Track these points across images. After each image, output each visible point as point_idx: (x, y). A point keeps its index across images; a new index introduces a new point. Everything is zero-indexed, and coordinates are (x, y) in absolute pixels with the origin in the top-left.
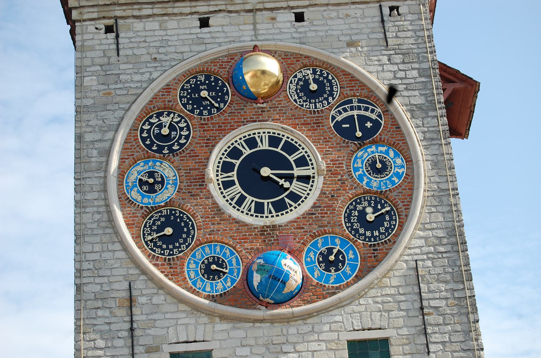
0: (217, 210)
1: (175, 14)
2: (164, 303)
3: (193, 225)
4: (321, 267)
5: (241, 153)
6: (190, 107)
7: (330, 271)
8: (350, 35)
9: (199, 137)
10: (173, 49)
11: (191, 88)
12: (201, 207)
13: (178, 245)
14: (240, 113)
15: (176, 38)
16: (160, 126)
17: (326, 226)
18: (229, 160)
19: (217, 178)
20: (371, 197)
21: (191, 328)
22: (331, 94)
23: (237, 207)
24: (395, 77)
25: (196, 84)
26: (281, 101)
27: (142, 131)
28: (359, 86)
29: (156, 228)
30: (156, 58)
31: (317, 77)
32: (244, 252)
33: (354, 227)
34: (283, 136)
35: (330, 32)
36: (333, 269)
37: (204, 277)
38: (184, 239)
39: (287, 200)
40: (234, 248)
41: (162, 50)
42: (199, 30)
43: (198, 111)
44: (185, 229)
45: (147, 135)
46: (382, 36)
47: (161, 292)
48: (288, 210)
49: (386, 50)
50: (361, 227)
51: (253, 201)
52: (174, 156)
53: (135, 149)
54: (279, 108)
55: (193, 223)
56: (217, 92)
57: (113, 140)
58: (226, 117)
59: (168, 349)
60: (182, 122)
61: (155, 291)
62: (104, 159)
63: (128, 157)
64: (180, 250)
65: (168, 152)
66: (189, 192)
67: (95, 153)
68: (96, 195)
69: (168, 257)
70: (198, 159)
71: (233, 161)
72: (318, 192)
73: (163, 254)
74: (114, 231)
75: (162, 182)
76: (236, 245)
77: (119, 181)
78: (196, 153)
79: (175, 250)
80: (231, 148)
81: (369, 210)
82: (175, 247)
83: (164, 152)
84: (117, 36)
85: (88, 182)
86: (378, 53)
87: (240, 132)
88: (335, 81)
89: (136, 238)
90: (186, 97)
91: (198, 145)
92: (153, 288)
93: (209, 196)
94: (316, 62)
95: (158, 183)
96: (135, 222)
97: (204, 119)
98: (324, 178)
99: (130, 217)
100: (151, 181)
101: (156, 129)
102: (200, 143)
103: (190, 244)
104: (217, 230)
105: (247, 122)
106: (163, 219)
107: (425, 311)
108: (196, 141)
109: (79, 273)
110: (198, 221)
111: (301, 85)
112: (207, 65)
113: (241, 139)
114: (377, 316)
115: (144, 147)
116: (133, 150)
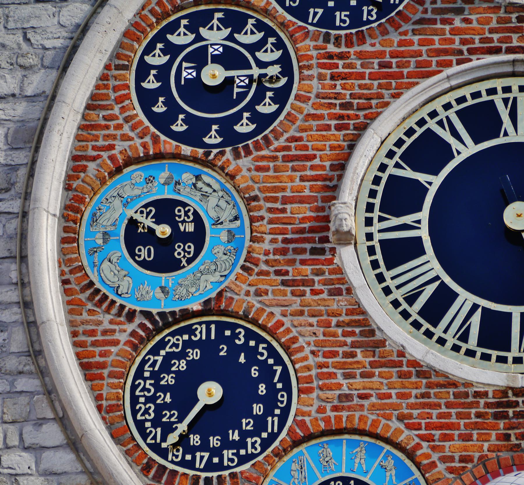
0: (362, 333)
3: (285, 377)
5: (447, 153)
9: (318, 96)
12: (314, 320)
13: (236, 437)
14: (449, 22)
16: (199, 58)
18: (408, 173)
19: (369, 229)
23: (426, 325)
27: (143, 70)
32: (441, 467)
38: (256, 418)
40: (411, 455)
43: (320, 11)
44: (262, 389)
45: (156, 85)
51: (475, 307)
52: (237, 155)
53: (119, 127)
55: (285, 370)
57: (53, 97)
58: (405, 33)
60: (269, 46)
62: (22, 157)
63: (95, 153)
64: (243, 452)
66: (278, 273)
69: (204, 475)
70: (312, 168)
71: (422, 177)
73: (191, 465)
74: (44, 385)
75: (198, 238)
76: (418, 446)
77: (66, 229)
78: (306, 148)
80: (416, 136)
82: (227, 444)
83: (206, 140)
87: (447, 85)
89: (107, 410)
91: (314, 123)
93: (340, 286)
95: (185, 237)
96: (109, 359)
97: (338, 38)
99: (95, 344)
100: (163, 231)
101: (185, 65)
102: (320, 117)
103: (273, 436)
104: (362, 397)
105: (471, 51)
106: (195, 354)
108: (308, 108)
110: (305, 361)
113: (447, 106)
115: (147, 123)
116: (112, 131)
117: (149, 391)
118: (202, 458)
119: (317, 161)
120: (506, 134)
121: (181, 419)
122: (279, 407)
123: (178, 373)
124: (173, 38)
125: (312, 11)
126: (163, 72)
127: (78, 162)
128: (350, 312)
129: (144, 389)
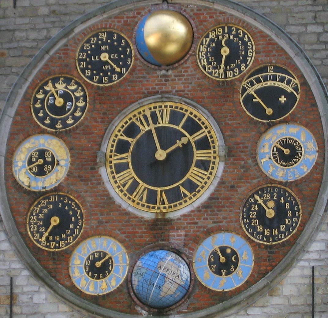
2: (44, 302)
4: (211, 268)
7: (220, 274)
11: (92, 49)
14: (141, 81)
17: (222, 222)
18: (125, 138)
20: (274, 188)
22: (245, 61)
23: (128, 195)
24: (318, 40)
25: (97, 44)
26: (188, 68)
28: (277, 51)
29: (43, 217)
30: (54, 11)
31: (232, 37)
33: (252, 224)
34: (186, 111)
36: (224, 272)
37: (88, 275)
39: (182, 189)
43: (97, 77)
47: (42, 290)
48: (182, 201)
49: (312, 5)
50: (259, 225)
51: (145, 188)
54: (185, 77)
56: (119, 54)
60: (79, 90)
61: (36, 288)
65: (61, 126)
70: (92, 137)
79: (61, 242)
81: (271, 204)
82: (61, 239)
83: (57, 126)
86: (304, 9)
88: (252, 44)
90: (85, 60)
92: (35, 285)
93: (100, 182)
94: (232, 19)
98: (225, 164)
101: (50, 98)
103: (77, 236)
106: (50, 207)
111: (212, 48)
112: (110, 21)
117: (35, 220)
118: (53, 244)
119: (93, 135)
120: (159, 123)
121: (46, 231)
122: (79, 225)
123: (45, 214)
124: (46, 88)
125: (94, 77)
126: (42, 101)
128: (104, 191)
129: (34, 220)
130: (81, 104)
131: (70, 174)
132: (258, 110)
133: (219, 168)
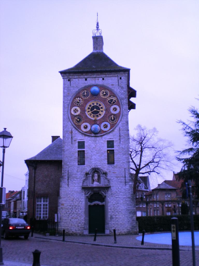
1: (81, 78)
6: (83, 97)
8: (112, 83)
10: (80, 85)
15: (81, 82)
21: (81, 137)
22: (108, 95)
30: (77, 87)
35: (109, 82)
41: (78, 85)
42: (85, 81)
46: (118, 83)
59: (78, 141)
67: (66, 105)
68: (66, 113)
72: (104, 114)
81: (113, 117)
84: (70, 82)
85: (65, 110)
93: (85, 114)
107: (121, 136)
109: (63, 127)
114: (112, 137)
127: (71, 106)
130: (82, 101)
131: (80, 112)
132: (110, 103)
133: (104, 112)
